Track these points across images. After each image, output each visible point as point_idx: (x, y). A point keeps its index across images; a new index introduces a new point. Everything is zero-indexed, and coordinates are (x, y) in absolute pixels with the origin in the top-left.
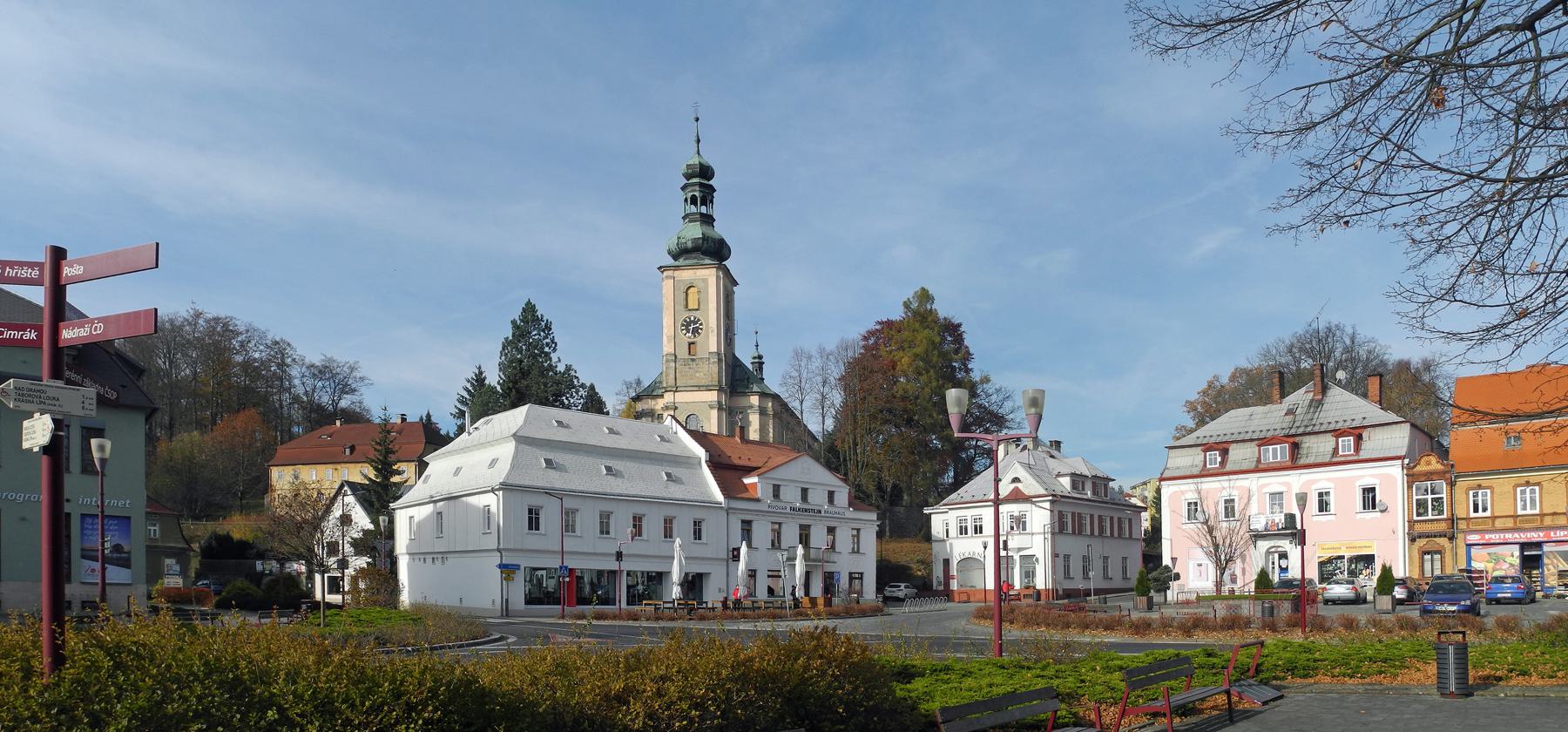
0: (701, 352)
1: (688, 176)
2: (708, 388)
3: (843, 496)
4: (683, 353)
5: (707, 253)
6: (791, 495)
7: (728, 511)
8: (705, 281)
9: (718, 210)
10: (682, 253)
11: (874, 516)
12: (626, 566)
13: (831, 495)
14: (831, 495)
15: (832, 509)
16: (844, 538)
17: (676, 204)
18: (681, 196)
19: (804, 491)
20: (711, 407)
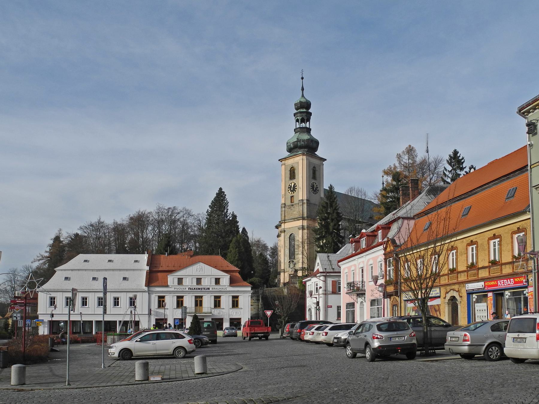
0: (296, 201)
1: (297, 109)
2: (297, 219)
3: (225, 279)
4: (288, 203)
5: (301, 147)
6: (188, 282)
7: (150, 293)
8: (298, 163)
9: (313, 124)
10: (293, 149)
11: (249, 289)
12: (54, 319)
13: (217, 281)
14: (217, 281)
15: (217, 287)
16: (226, 301)
17: (293, 124)
18: (293, 119)
19: (199, 281)
20: (299, 229)
